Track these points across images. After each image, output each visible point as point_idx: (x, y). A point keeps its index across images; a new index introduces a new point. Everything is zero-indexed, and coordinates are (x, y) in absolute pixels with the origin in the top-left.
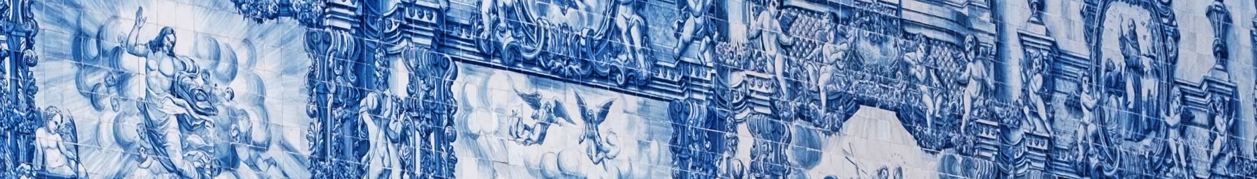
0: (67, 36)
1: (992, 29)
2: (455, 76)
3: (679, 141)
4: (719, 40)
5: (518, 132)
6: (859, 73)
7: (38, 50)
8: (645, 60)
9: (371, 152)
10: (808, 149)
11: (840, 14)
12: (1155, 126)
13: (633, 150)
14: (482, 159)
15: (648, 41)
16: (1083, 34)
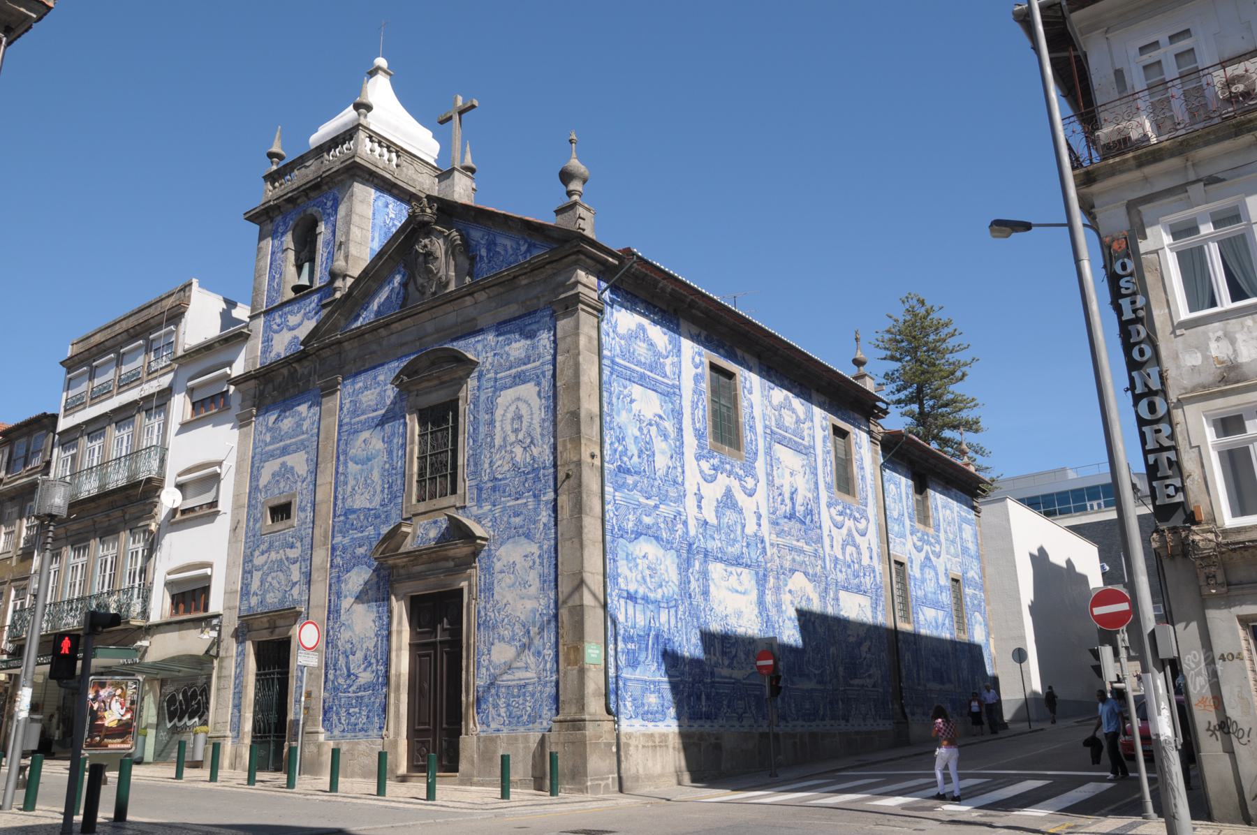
0: (625, 554)
5: (723, 578)
7: (618, 558)
12: (858, 576)
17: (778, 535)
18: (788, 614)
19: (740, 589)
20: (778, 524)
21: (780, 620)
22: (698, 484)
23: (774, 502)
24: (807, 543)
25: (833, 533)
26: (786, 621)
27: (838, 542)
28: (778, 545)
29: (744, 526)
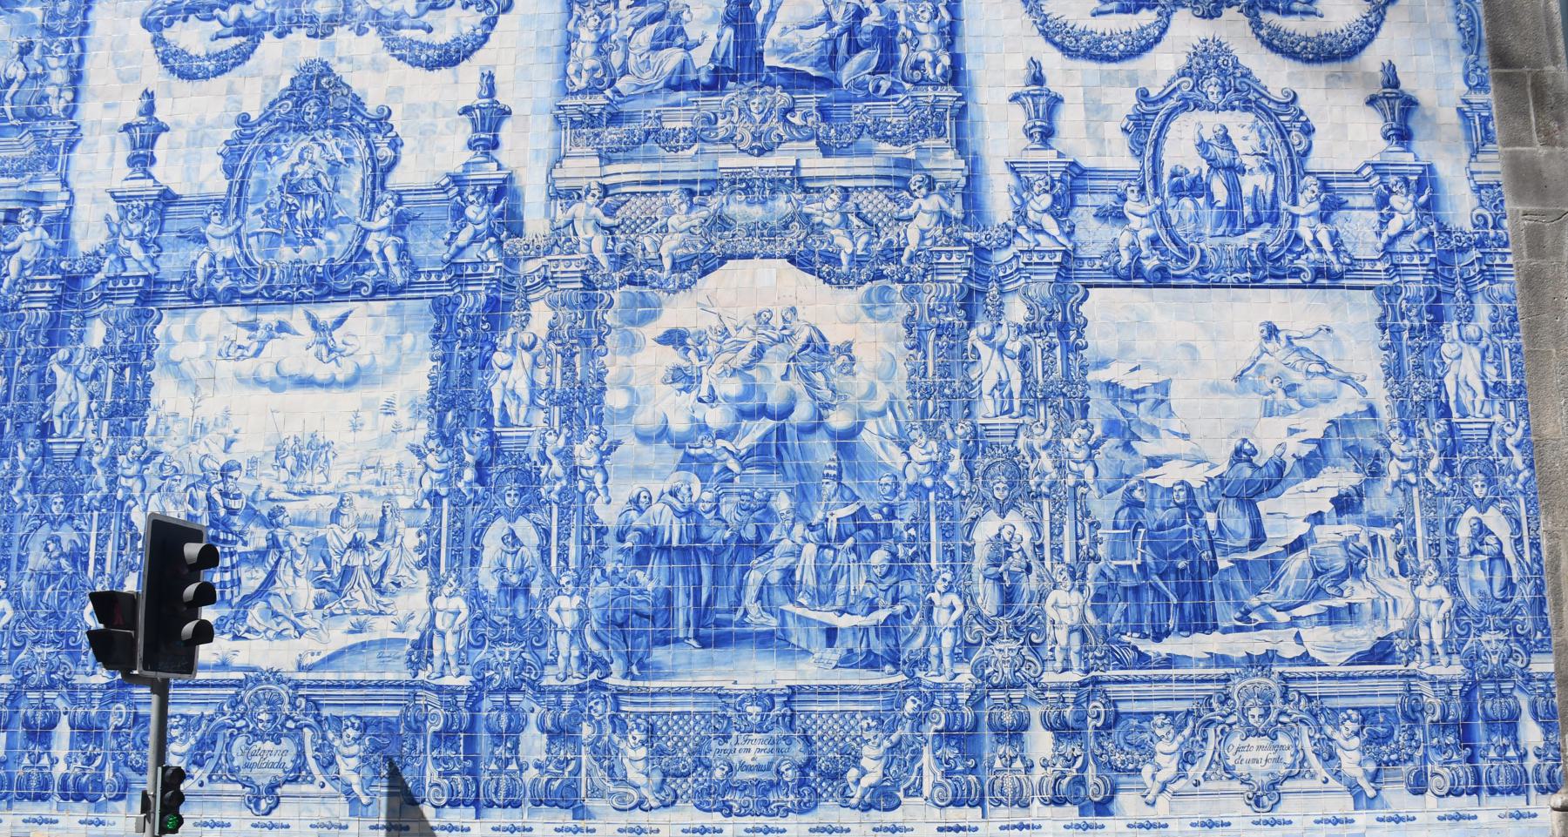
1: (961, 164)
2: (159, 322)
3: (443, 329)
4: (509, 237)
6: (726, 233)
9: (57, 392)
11: (698, 188)
14: (183, 379)
15: (407, 254)
17: (606, 158)
18: (646, 418)
19: (322, 372)
20: (615, 118)
22: (149, 95)
23: (598, 52)
24: (826, 151)
25: (1054, 84)
26: (630, 445)
27: (1096, 109)
28: (605, 189)
29: (380, 172)
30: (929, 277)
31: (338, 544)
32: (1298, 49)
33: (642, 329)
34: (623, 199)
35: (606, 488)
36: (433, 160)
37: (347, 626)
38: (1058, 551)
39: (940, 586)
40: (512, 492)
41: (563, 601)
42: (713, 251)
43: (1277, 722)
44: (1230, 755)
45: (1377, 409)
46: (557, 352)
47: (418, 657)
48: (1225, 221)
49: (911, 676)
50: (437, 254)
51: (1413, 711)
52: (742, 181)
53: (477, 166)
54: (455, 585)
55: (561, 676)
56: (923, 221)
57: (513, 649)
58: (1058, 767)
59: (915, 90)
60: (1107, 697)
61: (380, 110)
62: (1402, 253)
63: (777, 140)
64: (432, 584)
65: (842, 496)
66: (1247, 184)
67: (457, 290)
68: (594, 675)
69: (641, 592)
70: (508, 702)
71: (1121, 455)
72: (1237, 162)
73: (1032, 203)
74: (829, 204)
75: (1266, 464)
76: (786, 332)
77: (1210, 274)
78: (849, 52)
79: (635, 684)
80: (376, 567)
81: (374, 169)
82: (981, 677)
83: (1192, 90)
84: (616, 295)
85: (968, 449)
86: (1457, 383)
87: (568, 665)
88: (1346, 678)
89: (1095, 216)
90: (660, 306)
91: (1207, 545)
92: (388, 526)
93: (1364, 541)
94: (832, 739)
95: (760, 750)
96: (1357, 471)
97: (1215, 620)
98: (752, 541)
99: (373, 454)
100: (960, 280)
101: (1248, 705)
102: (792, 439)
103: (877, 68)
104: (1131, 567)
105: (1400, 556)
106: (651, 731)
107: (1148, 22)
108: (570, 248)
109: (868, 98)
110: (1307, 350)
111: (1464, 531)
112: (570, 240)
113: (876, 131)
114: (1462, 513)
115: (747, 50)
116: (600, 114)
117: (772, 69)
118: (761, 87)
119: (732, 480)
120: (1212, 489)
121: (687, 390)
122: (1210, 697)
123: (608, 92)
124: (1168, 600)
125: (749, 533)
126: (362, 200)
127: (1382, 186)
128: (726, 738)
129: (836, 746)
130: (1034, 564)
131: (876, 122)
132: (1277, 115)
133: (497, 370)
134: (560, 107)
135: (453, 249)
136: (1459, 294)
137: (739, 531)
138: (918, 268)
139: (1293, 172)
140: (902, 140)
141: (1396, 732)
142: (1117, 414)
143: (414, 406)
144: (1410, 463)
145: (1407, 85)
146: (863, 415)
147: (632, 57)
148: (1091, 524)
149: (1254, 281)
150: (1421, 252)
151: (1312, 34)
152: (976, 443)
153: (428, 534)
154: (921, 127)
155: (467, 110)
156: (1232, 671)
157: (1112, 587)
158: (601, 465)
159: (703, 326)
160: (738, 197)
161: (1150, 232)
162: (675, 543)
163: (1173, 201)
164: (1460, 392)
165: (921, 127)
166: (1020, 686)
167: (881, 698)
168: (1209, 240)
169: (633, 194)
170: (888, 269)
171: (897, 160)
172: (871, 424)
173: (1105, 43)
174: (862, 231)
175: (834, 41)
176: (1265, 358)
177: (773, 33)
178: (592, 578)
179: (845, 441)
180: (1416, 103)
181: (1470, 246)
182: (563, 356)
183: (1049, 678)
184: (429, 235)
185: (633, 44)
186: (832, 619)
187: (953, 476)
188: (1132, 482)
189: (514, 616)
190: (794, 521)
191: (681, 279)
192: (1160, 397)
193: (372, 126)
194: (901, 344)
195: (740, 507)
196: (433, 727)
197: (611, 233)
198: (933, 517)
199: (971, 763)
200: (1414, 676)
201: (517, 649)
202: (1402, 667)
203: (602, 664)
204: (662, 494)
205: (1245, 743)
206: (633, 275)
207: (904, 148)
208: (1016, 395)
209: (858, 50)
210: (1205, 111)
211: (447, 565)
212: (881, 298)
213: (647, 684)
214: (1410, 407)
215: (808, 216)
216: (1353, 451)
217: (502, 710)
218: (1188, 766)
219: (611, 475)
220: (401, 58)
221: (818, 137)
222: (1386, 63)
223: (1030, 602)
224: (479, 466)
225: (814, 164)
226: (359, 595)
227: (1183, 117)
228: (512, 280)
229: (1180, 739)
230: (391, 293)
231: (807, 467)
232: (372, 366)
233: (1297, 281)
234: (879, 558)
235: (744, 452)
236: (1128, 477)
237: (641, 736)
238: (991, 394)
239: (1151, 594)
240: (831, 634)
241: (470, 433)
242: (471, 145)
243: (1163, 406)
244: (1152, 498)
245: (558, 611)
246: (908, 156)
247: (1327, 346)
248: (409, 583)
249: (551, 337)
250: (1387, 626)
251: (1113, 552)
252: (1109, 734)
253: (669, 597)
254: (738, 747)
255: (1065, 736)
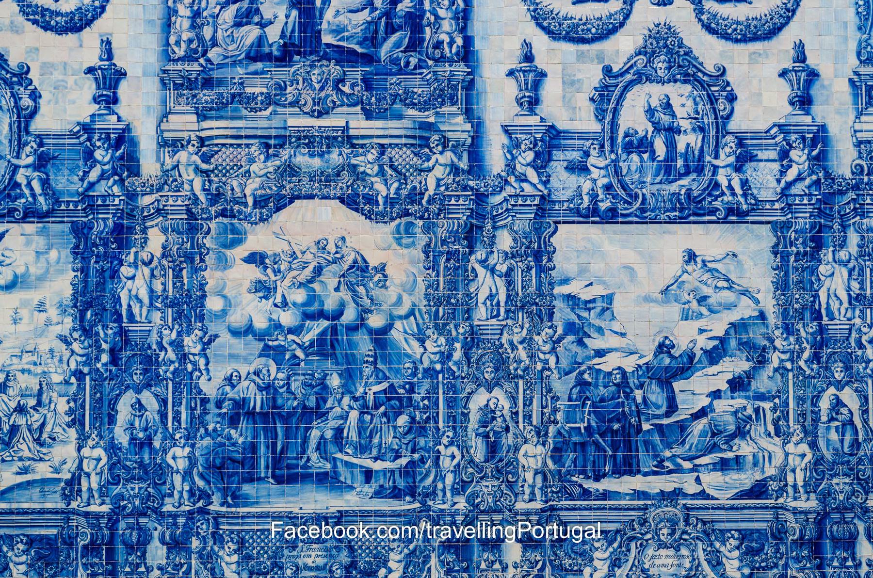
1: (468, 127)
3: (81, 247)
4: (129, 176)
6: (294, 178)
8: (46, 199)
10: (230, 236)
11: (272, 142)
13: (31, 258)
16: (593, 115)
17: (202, 116)
18: (237, 319)
20: (208, 83)
21: (188, 341)
23: (193, 27)
24: (369, 115)
25: (540, 62)
27: (570, 83)
28: (202, 141)
30: (442, 215)
31: (6, 409)
32: (729, 31)
33: (232, 251)
34: (216, 149)
35: (207, 370)
36: (65, 111)
37: (15, 469)
38: (528, 417)
39: (445, 440)
40: (138, 372)
41: (178, 451)
42: (284, 192)
43: (681, 538)
44: (646, 561)
45: (767, 314)
46: (169, 267)
47: (70, 491)
48: (663, 172)
49: (424, 503)
50: (73, 188)
51: (779, 532)
52: (305, 137)
53: (102, 118)
54: (97, 439)
55: (176, 504)
56: (439, 172)
57: (141, 485)
58: (525, 568)
59: (436, 66)
60: (560, 520)
61: (21, 66)
62: (795, 195)
63: (332, 105)
64: (79, 439)
65: (377, 376)
66: (682, 143)
67: (91, 217)
68: (200, 504)
69: (234, 444)
70: (138, 523)
71: (575, 348)
72: (675, 124)
73: (520, 158)
74: (370, 157)
75: (681, 355)
76: (338, 256)
77: (649, 213)
78: (386, 33)
79: (229, 510)
80: (36, 426)
81: (19, 116)
82: (472, 505)
83: (645, 66)
84: (213, 225)
85: (467, 343)
86: (829, 295)
87: (181, 497)
88: (732, 508)
89: (566, 168)
90: (245, 234)
91: (635, 413)
92: (44, 396)
93: (750, 411)
94: (368, 548)
95: (318, 556)
96: (748, 360)
97: (639, 466)
98: (312, 409)
99: (31, 341)
100: (465, 218)
101: (660, 526)
102: (342, 335)
103: (407, 47)
104: (580, 428)
105: (775, 423)
106: (242, 543)
107: (616, 10)
108: (176, 186)
109: (400, 72)
110: (717, 270)
111: (825, 404)
112: (176, 180)
113: (406, 99)
114: (824, 391)
115: (309, 30)
116: (196, 79)
117: (326, 44)
118: (319, 61)
119: (299, 364)
120: (640, 373)
121: (266, 298)
122: (633, 520)
123: (202, 61)
124: (605, 451)
125: (312, 402)
126: (10, 141)
127: (784, 143)
128: (294, 548)
129: (371, 552)
130: (511, 425)
131: (406, 92)
132: (709, 86)
133: (124, 280)
134: (164, 72)
135: (85, 184)
136: (836, 227)
137: (304, 401)
138: (434, 208)
139: (717, 132)
140: (424, 106)
141: (766, 547)
142: (574, 318)
143: (61, 306)
144: (788, 354)
145: (811, 61)
146: (392, 318)
147: (219, 31)
148: (552, 398)
149: (680, 218)
150: (810, 195)
151: (742, 18)
152: (473, 340)
153: (75, 401)
154: (440, 96)
155: (91, 70)
156: (649, 502)
157: (566, 443)
158: (203, 353)
159: (278, 250)
160: (302, 150)
161: (605, 181)
162: (258, 410)
163: (624, 156)
164: (830, 301)
165: (440, 96)
166: (499, 511)
167: (403, 519)
168: (649, 187)
169: (224, 145)
170: (413, 208)
171: (421, 122)
172: (398, 324)
173: (581, 27)
174: (394, 179)
175: (375, 23)
176: (685, 277)
177: (329, 15)
178: (199, 434)
179: (380, 337)
180: (818, 75)
181: (848, 189)
182: (174, 270)
183: (520, 506)
184: (66, 172)
185: (220, 20)
186: (369, 463)
187: (455, 363)
188: (583, 368)
189: (142, 462)
190: (343, 394)
191: (261, 213)
192: (605, 305)
193: (15, 79)
194: (421, 265)
195: (305, 384)
196: (82, 542)
197: (208, 176)
198: (441, 391)
199: (464, 565)
200: (782, 508)
201: (144, 485)
202: (773, 501)
203: (205, 496)
204: (249, 373)
205: (657, 553)
206: (225, 210)
207: (427, 113)
208: (502, 304)
209: (394, 31)
210: (654, 84)
211: (90, 425)
212: (407, 231)
213: (238, 510)
214: (791, 313)
215: (355, 166)
216: (747, 346)
217: (133, 529)
218: (616, 569)
219: (211, 360)
220: (35, 22)
221: (362, 103)
222: (798, 42)
223: (508, 452)
224: (112, 351)
225: (360, 125)
226: (24, 447)
227: (636, 88)
228: (132, 210)
229: (611, 549)
230: (39, 217)
231: (353, 355)
232: (26, 274)
233: (714, 218)
234: (402, 420)
235: (307, 344)
236: (580, 364)
237: (234, 547)
238: (484, 303)
239: (593, 448)
240: (368, 475)
241: (105, 327)
242: (96, 100)
243: (608, 313)
244: (597, 379)
245: (174, 458)
246: (429, 120)
247: (732, 268)
248: (61, 437)
249: (164, 256)
250: (763, 472)
251: (567, 418)
252: (561, 546)
253: (254, 448)
254: (302, 554)
255: (530, 546)
